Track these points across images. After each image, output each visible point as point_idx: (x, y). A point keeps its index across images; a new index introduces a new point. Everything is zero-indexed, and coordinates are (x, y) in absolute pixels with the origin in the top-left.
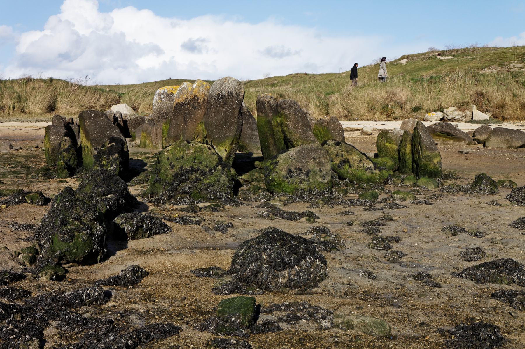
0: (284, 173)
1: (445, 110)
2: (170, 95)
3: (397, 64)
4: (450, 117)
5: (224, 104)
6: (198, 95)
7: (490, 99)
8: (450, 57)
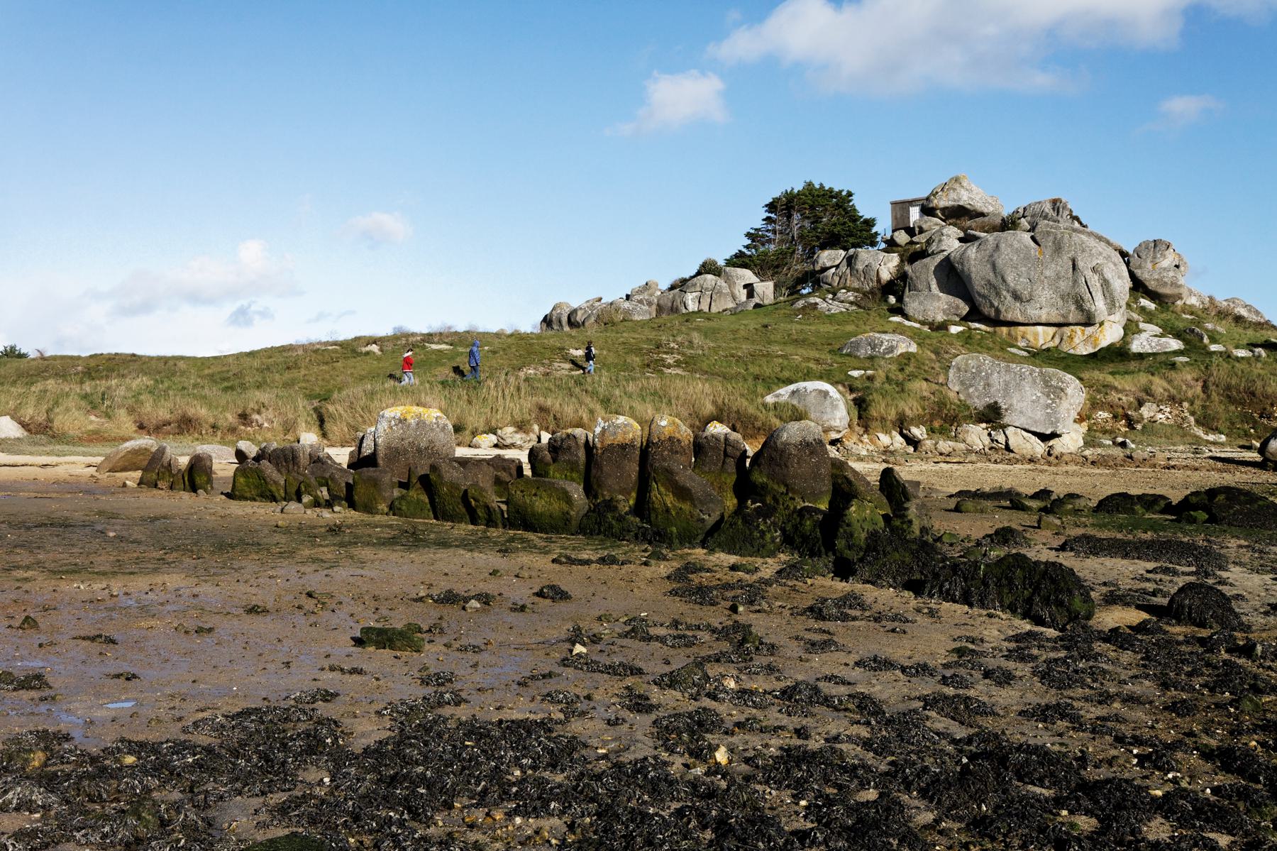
0: (918, 532)
1: (499, 432)
2: (402, 421)
3: (368, 353)
4: (509, 441)
5: (812, 453)
6: (677, 435)
7: (559, 416)
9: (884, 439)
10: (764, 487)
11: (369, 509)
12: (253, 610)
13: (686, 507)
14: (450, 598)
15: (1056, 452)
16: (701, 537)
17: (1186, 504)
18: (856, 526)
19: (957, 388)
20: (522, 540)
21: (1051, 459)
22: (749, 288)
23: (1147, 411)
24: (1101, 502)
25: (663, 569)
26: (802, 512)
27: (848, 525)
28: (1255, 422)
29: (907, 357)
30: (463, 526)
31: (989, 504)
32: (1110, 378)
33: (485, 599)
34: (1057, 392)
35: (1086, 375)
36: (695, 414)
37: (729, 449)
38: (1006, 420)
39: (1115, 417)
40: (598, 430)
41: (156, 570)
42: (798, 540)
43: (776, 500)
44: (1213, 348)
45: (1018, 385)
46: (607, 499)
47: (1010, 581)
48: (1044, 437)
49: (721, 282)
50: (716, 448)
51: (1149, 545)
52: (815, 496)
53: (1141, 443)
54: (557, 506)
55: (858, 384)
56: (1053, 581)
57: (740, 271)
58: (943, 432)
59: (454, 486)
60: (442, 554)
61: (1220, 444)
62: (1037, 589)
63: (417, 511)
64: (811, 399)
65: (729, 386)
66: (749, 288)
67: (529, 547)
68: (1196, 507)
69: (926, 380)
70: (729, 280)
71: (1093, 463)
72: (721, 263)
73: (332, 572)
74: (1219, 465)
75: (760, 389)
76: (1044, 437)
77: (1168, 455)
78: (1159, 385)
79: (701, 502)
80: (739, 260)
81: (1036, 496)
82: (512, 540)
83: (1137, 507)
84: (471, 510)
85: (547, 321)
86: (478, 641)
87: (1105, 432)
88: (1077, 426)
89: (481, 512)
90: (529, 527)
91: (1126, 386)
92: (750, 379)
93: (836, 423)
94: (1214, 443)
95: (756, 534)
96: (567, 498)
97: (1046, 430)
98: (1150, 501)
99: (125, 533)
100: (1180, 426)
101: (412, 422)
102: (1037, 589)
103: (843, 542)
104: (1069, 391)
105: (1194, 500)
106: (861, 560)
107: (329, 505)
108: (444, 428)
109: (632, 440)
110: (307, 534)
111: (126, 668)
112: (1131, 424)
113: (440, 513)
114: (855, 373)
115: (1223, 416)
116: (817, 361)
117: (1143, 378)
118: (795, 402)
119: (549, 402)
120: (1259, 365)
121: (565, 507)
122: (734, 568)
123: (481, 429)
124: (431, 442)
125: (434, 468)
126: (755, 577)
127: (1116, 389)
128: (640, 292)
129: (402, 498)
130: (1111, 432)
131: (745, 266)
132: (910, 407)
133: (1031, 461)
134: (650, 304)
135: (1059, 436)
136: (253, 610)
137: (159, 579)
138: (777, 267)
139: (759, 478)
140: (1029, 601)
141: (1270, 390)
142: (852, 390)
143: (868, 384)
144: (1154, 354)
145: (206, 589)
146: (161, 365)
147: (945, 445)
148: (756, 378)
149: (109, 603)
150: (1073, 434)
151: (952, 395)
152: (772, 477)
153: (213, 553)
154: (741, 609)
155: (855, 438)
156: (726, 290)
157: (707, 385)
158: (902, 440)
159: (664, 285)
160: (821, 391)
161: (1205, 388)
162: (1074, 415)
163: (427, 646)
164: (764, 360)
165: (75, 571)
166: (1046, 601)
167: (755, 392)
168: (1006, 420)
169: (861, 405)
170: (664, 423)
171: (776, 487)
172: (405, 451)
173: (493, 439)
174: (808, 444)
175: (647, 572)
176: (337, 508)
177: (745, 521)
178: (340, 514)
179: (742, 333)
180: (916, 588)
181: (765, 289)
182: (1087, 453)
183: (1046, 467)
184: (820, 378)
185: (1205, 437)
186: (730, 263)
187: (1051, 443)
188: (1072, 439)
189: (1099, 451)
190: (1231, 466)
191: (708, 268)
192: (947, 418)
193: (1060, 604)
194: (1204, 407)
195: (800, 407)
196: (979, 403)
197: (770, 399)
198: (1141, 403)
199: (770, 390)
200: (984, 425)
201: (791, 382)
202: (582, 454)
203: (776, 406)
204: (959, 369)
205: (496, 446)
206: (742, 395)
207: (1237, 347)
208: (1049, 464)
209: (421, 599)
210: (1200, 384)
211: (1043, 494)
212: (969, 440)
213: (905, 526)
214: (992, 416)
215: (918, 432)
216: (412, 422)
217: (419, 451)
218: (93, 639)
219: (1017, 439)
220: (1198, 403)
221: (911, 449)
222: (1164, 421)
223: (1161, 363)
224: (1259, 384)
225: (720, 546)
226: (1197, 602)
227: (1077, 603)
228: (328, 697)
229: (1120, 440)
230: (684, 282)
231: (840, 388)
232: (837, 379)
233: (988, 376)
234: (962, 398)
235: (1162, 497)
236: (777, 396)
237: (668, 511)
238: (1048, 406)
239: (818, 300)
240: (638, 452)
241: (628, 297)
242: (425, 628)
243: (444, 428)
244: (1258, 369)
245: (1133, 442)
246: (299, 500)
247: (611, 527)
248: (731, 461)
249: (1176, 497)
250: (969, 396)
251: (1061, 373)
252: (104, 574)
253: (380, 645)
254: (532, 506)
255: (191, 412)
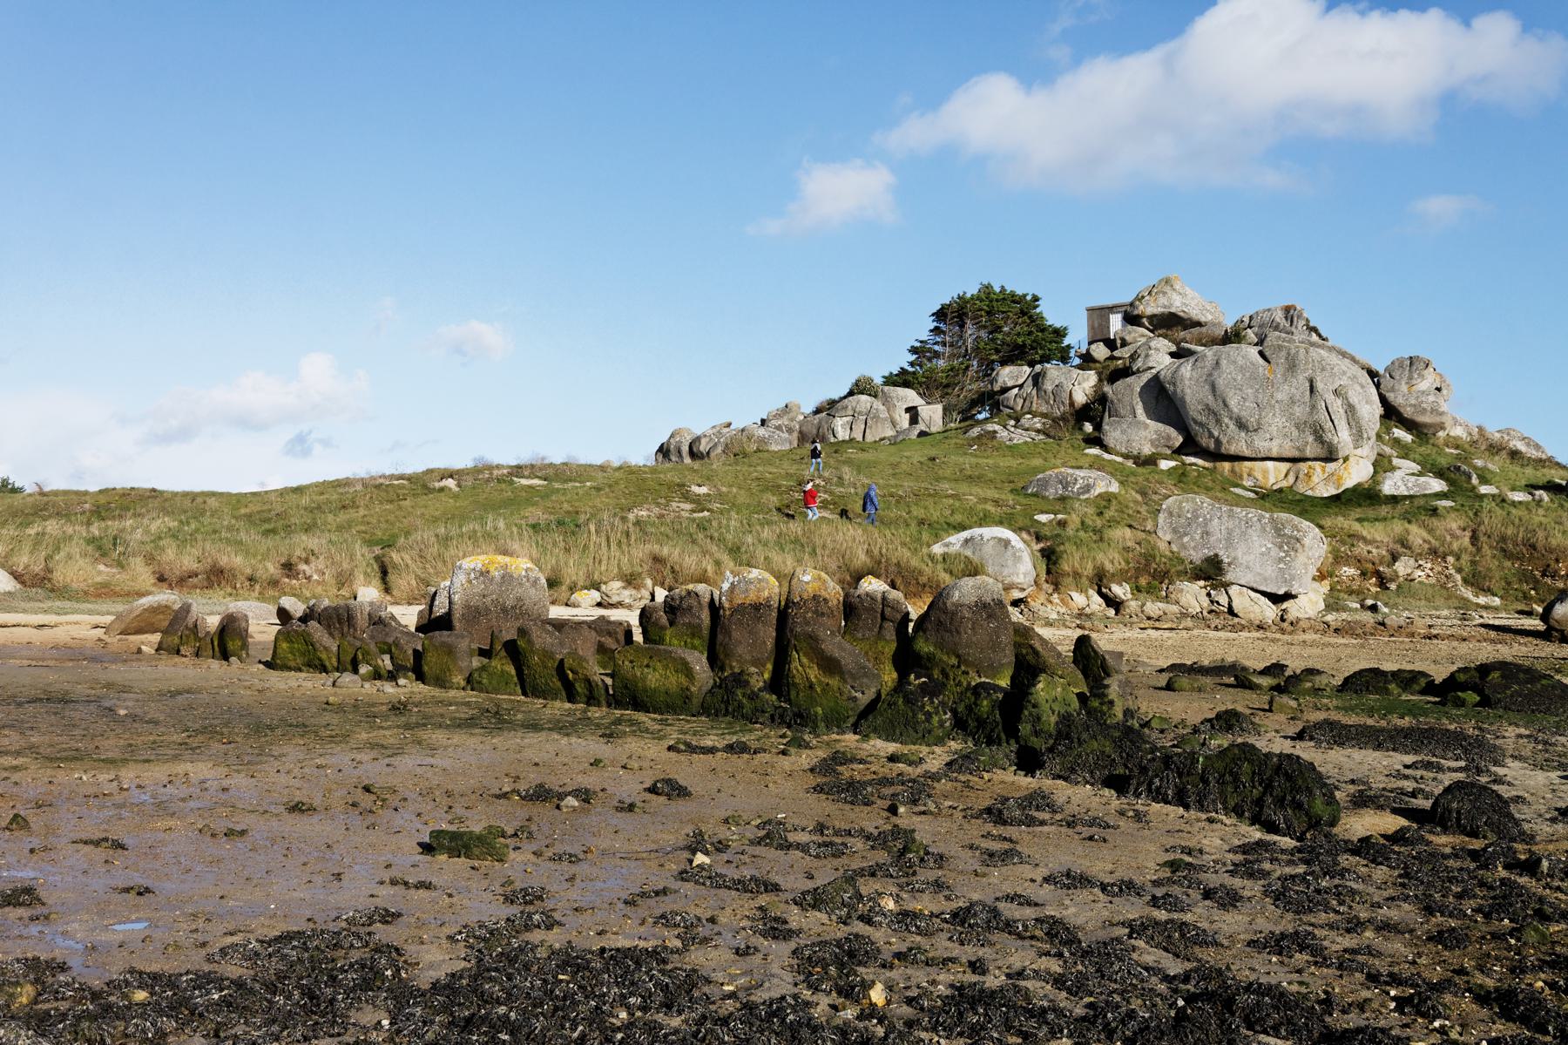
0: (1120, 716)
1: (603, 587)
2: (484, 573)
3: (442, 489)
4: (615, 599)
5: (990, 616)
6: (823, 593)
7: (677, 568)
8: (536, 482)
9: (1079, 599)
10: (930, 658)
11: (441, 682)
12: (296, 808)
13: (834, 682)
14: (541, 794)
15: (1290, 616)
16: (852, 720)
17: (1452, 684)
18: (1045, 707)
19: (1168, 537)
20: (632, 722)
21: (1285, 625)
22: (913, 412)
23: (1403, 567)
24: (1347, 680)
25: (805, 759)
26: (977, 690)
27: (1035, 706)
28: (1537, 581)
29: (1107, 498)
30: (558, 704)
31: (1208, 681)
32: (1357, 526)
33: (585, 796)
34: (1291, 543)
35: (1327, 522)
36: (845, 567)
37: (888, 611)
38: (1229, 577)
39: (1363, 574)
40: (726, 586)
41: (176, 758)
42: (972, 724)
43: (946, 676)
44: (1484, 489)
45: (1244, 533)
46: (740, 671)
47: (1236, 778)
48: (1276, 599)
49: (878, 404)
50: (871, 610)
51: (1406, 733)
52: (994, 670)
53: (1395, 606)
54: (674, 681)
55: (1046, 531)
56: (1289, 777)
57: (901, 391)
58: (1150, 590)
59: (547, 654)
60: (532, 738)
61: (1493, 608)
62: (1268, 787)
63: (501, 684)
64: (988, 549)
65: (887, 532)
66: (913, 412)
67: (640, 730)
68: (1464, 687)
69: (1130, 526)
70: (887, 401)
71: (1336, 631)
72: (878, 380)
73: (395, 761)
74: (1493, 634)
75: (925, 536)
76: (1276, 599)
77: (1429, 621)
78: (1417, 535)
79: (854, 677)
80: (901, 379)
81: (1266, 672)
82: (618, 722)
83: (1392, 687)
84: (569, 685)
85: (664, 451)
86: (576, 849)
87: (1351, 592)
88: (1316, 585)
89: (580, 688)
90: (638, 704)
91: (1377, 535)
92: (913, 524)
93: (1020, 579)
94: (1486, 607)
95: (921, 717)
96: (687, 670)
97: (1279, 589)
98: (1408, 679)
99: (138, 711)
100: (1443, 586)
101: (496, 574)
102: (1268, 787)
103: (1029, 727)
104: (1306, 541)
105: (1462, 677)
106: (1051, 750)
107: (392, 677)
108: (535, 582)
109: (768, 599)
110: (366, 713)
111: (138, 880)
112: (1382, 582)
113: (528, 687)
114: (1043, 518)
115: (1497, 575)
116: (996, 502)
117: (1398, 527)
118: (969, 553)
119: (665, 551)
120: (1541, 512)
121: (683, 679)
122: (893, 758)
123: (581, 583)
124: (519, 599)
125: (522, 632)
126: (919, 770)
127: (1364, 539)
128: (778, 415)
129: (483, 668)
130: (1358, 592)
131: (906, 384)
132: (1111, 560)
133: (1260, 627)
134: (790, 431)
135: (1294, 597)
136: (296, 808)
137: (180, 768)
138: (947, 386)
139: (924, 646)
140: (1259, 802)
141: (1554, 542)
142: (1038, 538)
143: (1058, 531)
144: (1411, 497)
145: (239, 781)
146: (187, 503)
147: (1154, 608)
148: (921, 522)
149: (118, 798)
150: (1312, 595)
151: (1162, 546)
152: (940, 645)
153: (247, 736)
154: (902, 810)
155: (1042, 598)
156: (884, 415)
157: (860, 531)
158: (1100, 600)
159: (808, 408)
160: (1000, 540)
161: (1474, 538)
162: (1313, 571)
163: (512, 855)
164: (931, 500)
165: (76, 757)
166: (1280, 802)
167: (919, 540)
168: (1229, 577)
169: (1050, 556)
170: (807, 578)
171: (945, 658)
172: (487, 610)
173: (595, 596)
174: (985, 606)
175: (785, 763)
176: (402, 681)
177: (907, 701)
178: (407, 687)
179: (904, 467)
180: (1118, 784)
181: (933, 414)
182: (1329, 618)
183: (1278, 636)
184: (1000, 523)
185: (1475, 600)
186: (891, 381)
187: (1285, 605)
188: (1310, 602)
189: (1344, 615)
190: (1508, 636)
191: (861, 387)
192: (1154, 574)
193: (1298, 806)
194: (1473, 563)
195: (975, 559)
196: (1196, 556)
197: (937, 549)
198: (1395, 558)
199: (937, 538)
200: (1202, 583)
201: (964, 528)
202: (705, 616)
203: (945, 557)
204: (1171, 514)
205: (599, 605)
206: (904, 544)
207: (1513, 489)
208: (1283, 631)
209: (505, 796)
210: (1468, 534)
211: (1275, 669)
212: (1183, 601)
213: (1105, 708)
214: (1211, 571)
215: (1120, 591)
216: (496, 574)
217: (504, 610)
218: (97, 843)
219: (1243, 601)
220: (1465, 558)
221: (1112, 612)
222: (1423, 579)
223: (1420, 508)
224: (1541, 534)
225: (875, 730)
226: (1467, 806)
227: (1319, 805)
228: (388, 917)
229: (1369, 602)
230: (832, 403)
231: (1025, 535)
232: (1020, 524)
233: (1206, 523)
234: (1175, 548)
235: (1423, 674)
236: (947, 545)
237: (811, 687)
238: (1281, 560)
239: (997, 427)
240: (774, 614)
241: (763, 422)
242: (510, 831)
243: (535, 582)
244: (1539, 517)
245: (1386, 605)
246: (356, 671)
247: (740, 706)
248: (889, 626)
249: (1440, 674)
250: (1184, 547)
251: (1297, 519)
252: (112, 762)
253: (454, 853)
254: (644, 679)
255: (224, 561)
